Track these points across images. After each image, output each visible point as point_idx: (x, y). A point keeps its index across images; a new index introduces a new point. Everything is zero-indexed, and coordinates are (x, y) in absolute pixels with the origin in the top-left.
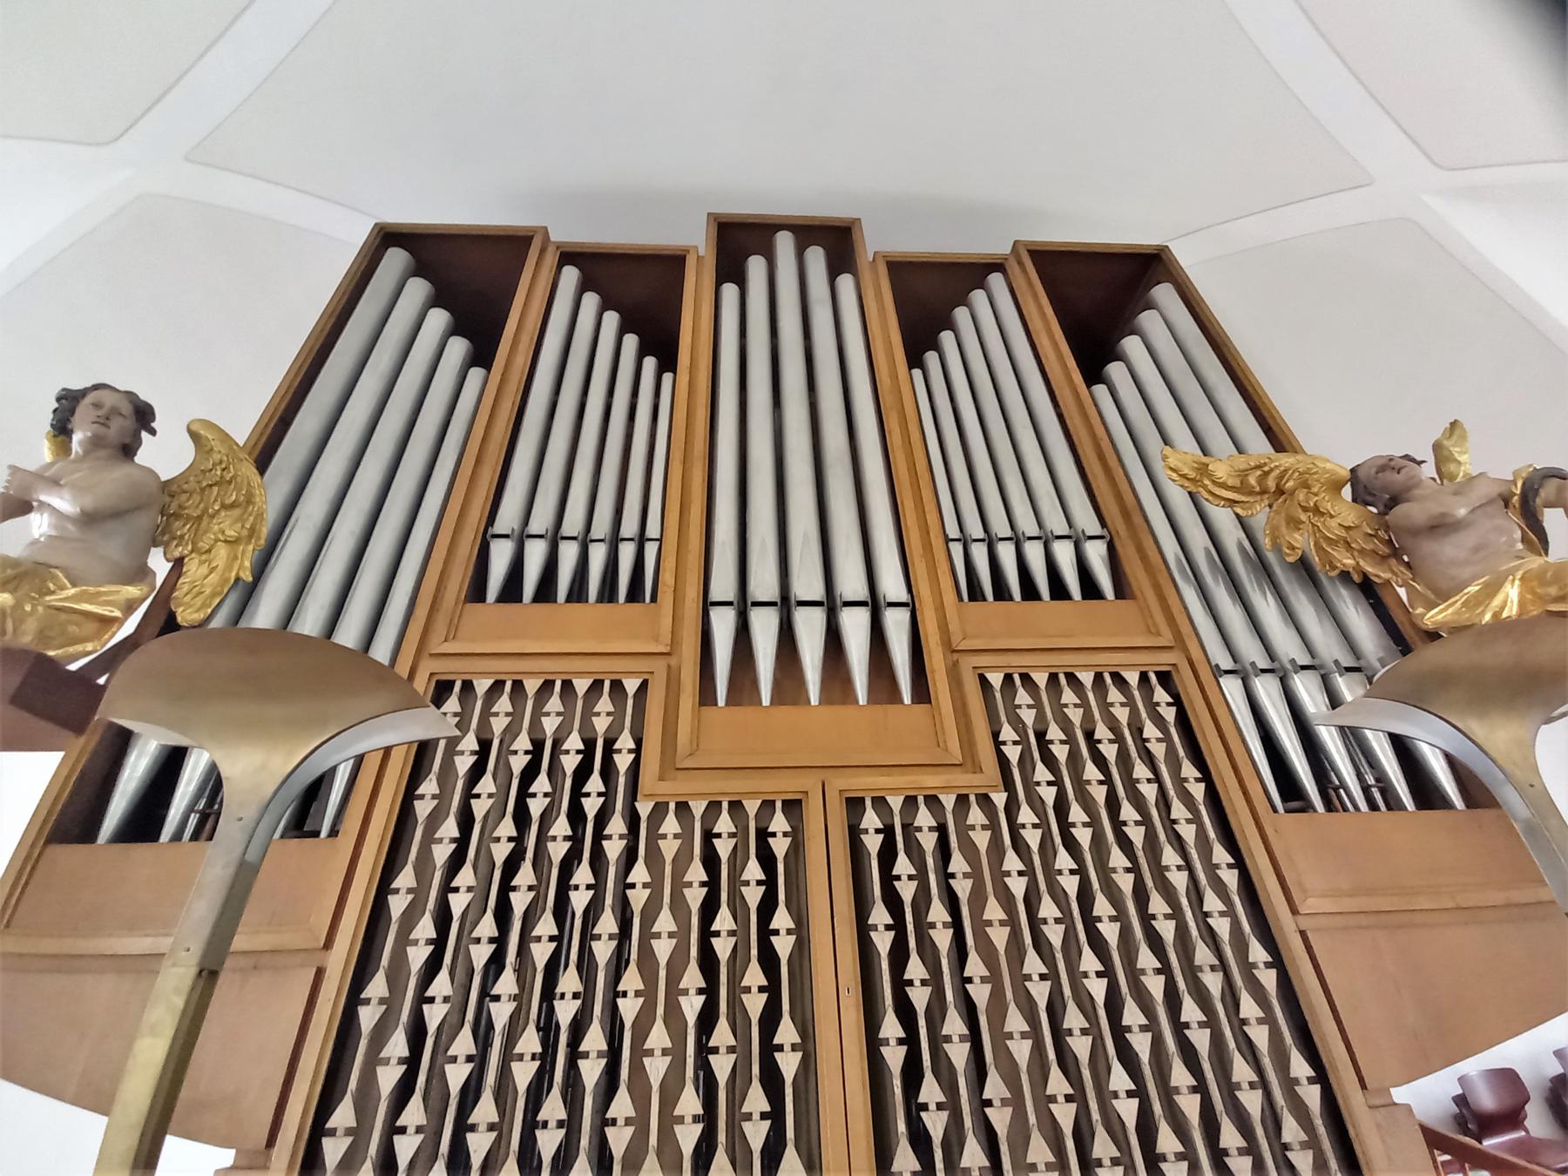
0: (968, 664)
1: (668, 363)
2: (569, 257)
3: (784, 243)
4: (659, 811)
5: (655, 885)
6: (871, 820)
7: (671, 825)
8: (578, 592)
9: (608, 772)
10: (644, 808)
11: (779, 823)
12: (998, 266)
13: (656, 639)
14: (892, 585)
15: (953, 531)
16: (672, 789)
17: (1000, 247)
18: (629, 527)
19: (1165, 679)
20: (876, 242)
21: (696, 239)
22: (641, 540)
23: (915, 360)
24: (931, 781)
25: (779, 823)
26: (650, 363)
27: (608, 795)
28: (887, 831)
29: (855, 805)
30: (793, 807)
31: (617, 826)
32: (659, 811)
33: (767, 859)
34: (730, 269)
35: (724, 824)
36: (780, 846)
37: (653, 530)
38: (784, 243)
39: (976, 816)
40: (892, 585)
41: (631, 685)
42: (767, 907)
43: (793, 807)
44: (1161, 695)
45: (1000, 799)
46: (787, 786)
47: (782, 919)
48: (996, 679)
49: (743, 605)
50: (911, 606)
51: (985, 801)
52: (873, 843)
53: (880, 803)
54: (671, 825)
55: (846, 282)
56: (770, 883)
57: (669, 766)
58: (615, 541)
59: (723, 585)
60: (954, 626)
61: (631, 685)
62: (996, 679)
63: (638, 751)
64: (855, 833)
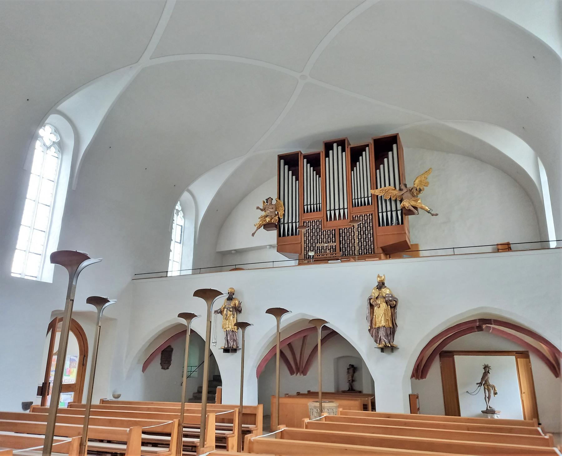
0: (351, 215)
4: (323, 231)
6: (341, 230)
8: (314, 211)
9: (319, 228)
10: (322, 231)
11: (333, 231)
13: (322, 215)
16: (324, 229)
18: (318, 203)
19: (372, 214)
23: (352, 170)
27: (319, 230)
29: (340, 229)
30: (335, 230)
31: (320, 233)
32: (323, 231)
34: (327, 155)
39: (350, 229)
40: (346, 207)
41: (320, 220)
42: (332, 238)
43: (335, 230)
44: (371, 216)
46: (334, 228)
48: (354, 216)
49: (330, 210)
51: (351, 228)
53: (342, 229)
56: (333, 236)
57: (324, 228)
59: (328, 209)
60: (351, 210)
61: (320, 220)
62: (354, 216)
63: (321, 226)
64: (340, 232)
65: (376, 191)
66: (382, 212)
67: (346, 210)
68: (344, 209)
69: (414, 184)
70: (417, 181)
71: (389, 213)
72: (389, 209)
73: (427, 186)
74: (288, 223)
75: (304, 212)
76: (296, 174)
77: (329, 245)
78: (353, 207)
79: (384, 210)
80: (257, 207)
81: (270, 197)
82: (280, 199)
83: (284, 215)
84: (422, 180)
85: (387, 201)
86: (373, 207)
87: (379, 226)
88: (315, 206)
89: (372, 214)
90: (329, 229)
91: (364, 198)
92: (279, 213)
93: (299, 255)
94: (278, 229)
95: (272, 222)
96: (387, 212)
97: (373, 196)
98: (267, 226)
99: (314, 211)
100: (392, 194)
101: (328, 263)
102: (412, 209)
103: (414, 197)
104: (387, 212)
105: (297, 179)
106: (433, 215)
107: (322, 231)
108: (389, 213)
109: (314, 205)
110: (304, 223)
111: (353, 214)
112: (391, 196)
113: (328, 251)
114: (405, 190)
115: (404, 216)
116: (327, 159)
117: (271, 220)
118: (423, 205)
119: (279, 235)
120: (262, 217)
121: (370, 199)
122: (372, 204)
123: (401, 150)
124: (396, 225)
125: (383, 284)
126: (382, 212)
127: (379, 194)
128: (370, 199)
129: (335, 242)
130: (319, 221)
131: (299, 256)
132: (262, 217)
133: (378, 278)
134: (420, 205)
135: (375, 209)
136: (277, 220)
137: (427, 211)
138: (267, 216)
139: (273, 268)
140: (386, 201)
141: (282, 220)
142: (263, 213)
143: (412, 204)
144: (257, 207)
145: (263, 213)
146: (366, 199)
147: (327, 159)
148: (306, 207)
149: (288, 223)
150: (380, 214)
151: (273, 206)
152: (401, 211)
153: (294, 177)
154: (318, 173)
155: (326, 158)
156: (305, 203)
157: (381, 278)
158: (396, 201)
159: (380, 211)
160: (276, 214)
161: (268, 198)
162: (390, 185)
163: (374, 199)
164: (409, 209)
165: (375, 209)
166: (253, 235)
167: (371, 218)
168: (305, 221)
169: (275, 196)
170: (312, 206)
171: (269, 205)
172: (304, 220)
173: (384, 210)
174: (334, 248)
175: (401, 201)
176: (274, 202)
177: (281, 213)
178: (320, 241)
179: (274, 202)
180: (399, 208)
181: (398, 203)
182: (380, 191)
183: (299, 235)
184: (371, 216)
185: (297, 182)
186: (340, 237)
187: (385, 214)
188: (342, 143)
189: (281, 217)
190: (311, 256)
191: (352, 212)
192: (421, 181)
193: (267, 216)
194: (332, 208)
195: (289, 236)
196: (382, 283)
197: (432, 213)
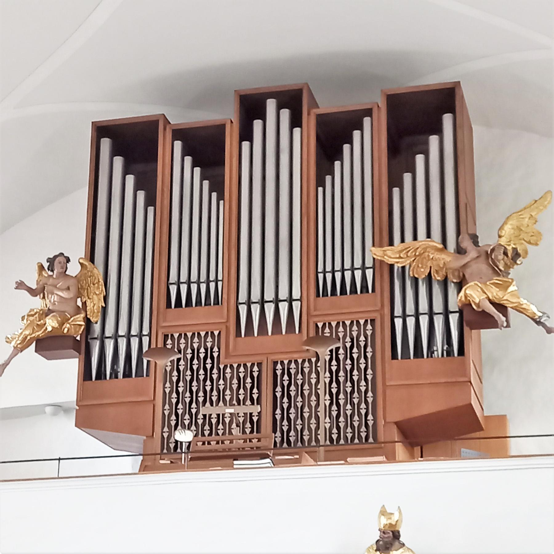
1: (221, 197)
4: (225, 367)
5: (225, 384)
6: (279, 367)
7: (228, 370)
8: (199, 303)
9: (212, 358)
10: (222, 367)
11: (256, 369)
16: (228, 362)
18: (212, 277)
19: (373, 321)
22: (216, 281)
24: (295, 356)
25: (256, 369)
26: (214, 195)
27: (213, 363)
28: (283, 369)
29: (275, 363)
30: (259, 365)
31: (215, 371)
32: (225, 367)
33: (252, 377)
35: (242, 369)
36: (255, 374)
39: (307, 364)
40: (296, 294)
41: (216, 333)
42: (252, 388)
43: (259, 365)
44: (369, 327)
45: (314, 360)
47: (255, 391)
48: (320, 325)
49: (249, 303)
51: (310, 361)
52: (279, 372)
53: (282, 363)
54: (228, 370)
55: (297, 131)
56: (253, 383)
57: (227, 355)
58: (208, 282)
59: (243, 297)
60: (312, 307)
61: (216, 333)
62: (320, 325)
63: (219, 352)
64: (275, 370)
66: (404, 317)
67: (296, 305)
68: (290, 300)
69: (500, 237)
70: (508, 228)
71: (424, 321)
72: (424, 306)
73: (537, 244)
74: (116, 337)
75: (169, 305)
77: (242, 410)
78: (318, 295)
80: (17, 282)
81: (62, 254)
82: (92, 259)
83: (104, 310)
84: (522, 225)
85: (420, 283)
87: (394, 356)
88: (203, 287)
89: (373, 321)
90: (242, 360)
92: (88, 304)
93: (145, 438)
94: (83, 356)
96: (417, 315)
97: (377, 265)
99: (199, 303)
100: (435, 263)
101: (231, 467)
102: (492, 310)
103: (499, 275)
104: (417, 315)
105: (150, 201)
107: (222, 367)
108: (424, 321)
109: (199, 283)
110: (166, 337)
111: (316, 319)
112: (431, 267)
114: (472, 253)
115: (466, 329)
117: (62, 324)
118: (523, 301)
119: (86, 374)
120: (33, 315)
121: (369, 273)
122: (373, 290)
123: (465, 132)
124: (443, 355)
125: (396, 535)
126: (404, 317)
127: (397, 260)
128: (369, 273)
131: (144, 441)
132: (33, 315)
133: (379, 518)
134: (514, 301)
135: (382, 306)
136: (81, 325)
137: (533, 319)
138: (47, 313)
139: (59, 478)
140: (415, 281)
141: (97, 328)
142: (37, 303)
143: (491, 298)
144: (17, 282)
145: (37, 303)
146: (358, 274)
148: (173, 290)
149: (116, 337)
150: (398, 323)
151: (71, 283)
153: (141, 195)
157: (390, 518)
158: (445, 284)
159: (398, 311)
160: (79, 307)
161: (55, 257)
162: (429, 236)
163: (382, 276)
164: (483, 311)
165: (382, 306)
167: (369, 333)
168: (169, 332)
170: (194, 287)
171: (58, 278)
172: (166, 331)
174: (255, 419)
175: (460, 286)
176: (73, 269)
178: (214, 399)
179: (73, 269)
180: (453, 305)
181: (452, 289)
182: (401, 251)
184: (369, 327)
185: (151, 209)
186: (275, 386)
187: (411, 322)
189: (96, 319)
190: (181, 443)
192: (519, 229)
193: (47, 313)
194: (256, 296)
195: (117, 377)
196: (391, 533)
197: (548, 324)
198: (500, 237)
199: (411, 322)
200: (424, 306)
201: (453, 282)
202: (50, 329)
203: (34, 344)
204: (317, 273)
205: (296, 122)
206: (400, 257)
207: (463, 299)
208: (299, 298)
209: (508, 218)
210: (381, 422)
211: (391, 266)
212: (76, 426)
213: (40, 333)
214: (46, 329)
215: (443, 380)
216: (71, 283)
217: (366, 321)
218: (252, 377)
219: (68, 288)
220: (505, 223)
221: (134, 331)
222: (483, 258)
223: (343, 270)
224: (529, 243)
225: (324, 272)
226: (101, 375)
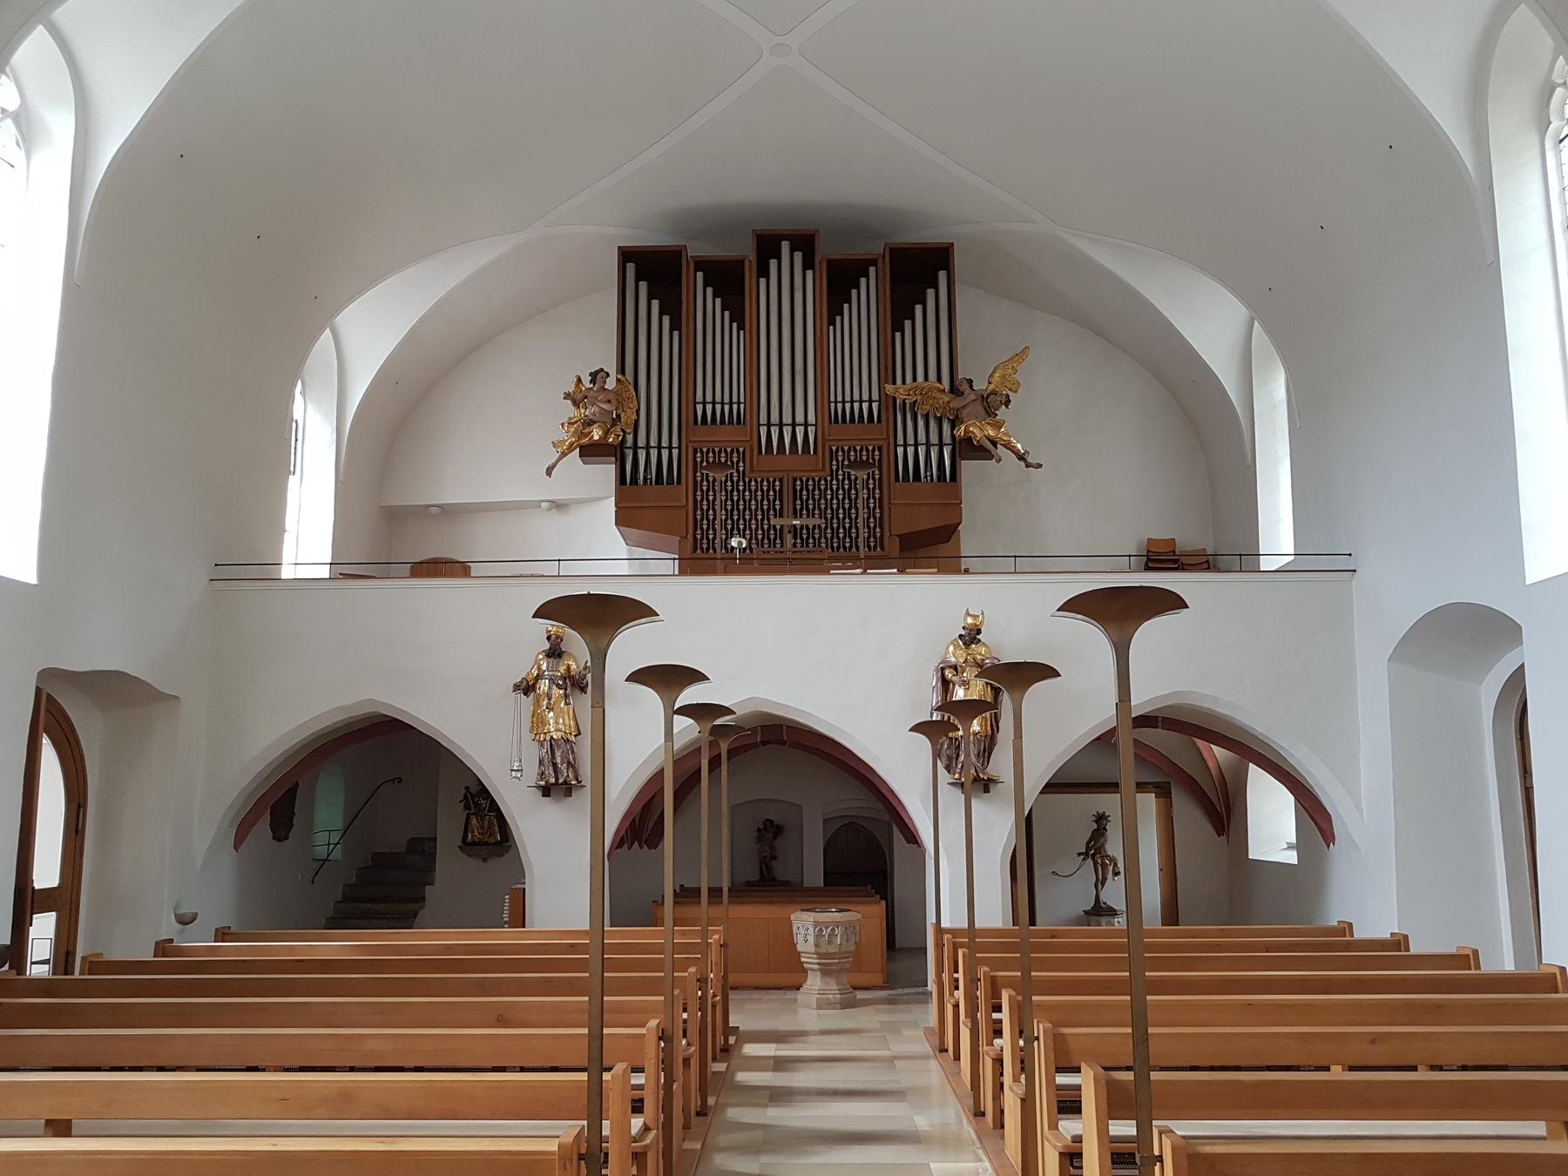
0: (827, 444)
2: (701, 264)
3: (785, 246)
4: (750, 481)
6: (798, 483)
8: (723, 422)
10: (747, 480)
11: (777, 483)
12: (874, 262)
14: (811, 418)
15: (832, 399)
17: (876, 248)
19: (880, 449)
20: (824, 251)
21: (746, 250)
22: (739, 403)
34: (763, 272)
37: (742, 400)
38: (785, 246)
40: (811, 418)
41: (741, 450)
42: (774, 500)
43: (781, 480)
44: (877, 453)
45: (829, 479)
48: (834, 448)
50: (816, 425)
51: (826, 480)
55: (809, 273)
57: (752, 470)
58: (731, 403)
59: (763, 420)
61: (741, 450)
62: (834, 448)
65: (901, 391)
66: (905, 445)
67: (811, 430)
69: (990, 383)
72: (922, 437)
73: (1016, 392)
74: (648, 447)
76: (673, 308)
78: (830, 422)
79: (911, 440)
80: (565, 393)
82: (623, 372)
83: (637, 422)
85: (919, 417)
86: (885, 429)
88: (727, 408)
89: (880, 449)
90: (765, 475)
91: (861, 401)
92: (622, 416)
93: (678, 538)
95: (611, 440)
97: (883, 398)
98: (590, 452)
99: (723, 422)
103: (990, 416)
104: (916, 445)
106: (1028, 465)
107: (747, 480)
109: (723, 404)
110: (695, 451)
111: (831, 443)
113: (789, 539)
116: (763, 281)
117: (606, 433)
120: (573, 423)
121: (875, 406)
122: (879, 421)
126: (905, 445)
128: (875, 406)
129: (781, 516)
130: (738, 451)
131: (680, 541)
132: (573, 423)
136: (619, 436)
138: (589, 423)
141: (630, 438)
146: (865, 406)
147: (763, 281)
148: (699, 408)
149: (648, 447)
152: (951, 447)
154: (738, 317)
155: (759, 277)
156: (699, 397)
158: (939, 421)
159: (900, 441)
166: (549, 471)
169: (611, 368)
170: (718, 407)
171: (598, 391)
173: (911, 440)
176: (611, 384)
177: (628, 417)
179: (611, 384)
180: (947, 438)
183: (679, 482)
184: (877, 453)
185: (676, 333)
186: (795, 500)
188: (805, 243)
191: (829, 435)
192: (1003, 377)
193: (589, 423)
195: (636, 484)
198: (990, 383)
199: (910, 450)
200: (922, 437)
201: (948, 418)
202: (596, 438)
203: (578, 449)
204: (830, 402)
205: (808, 264)
206: (909, 395)
207: (962, 434)
208: (814, 423)
209: (996, 368)
210: (887, 534)
211: (895, 399)
212: (616, 524)
213: (585, 441)
214: (592, 437)
215: (940, 502)
216: (611, 397)
217: (874, 447)
218: (774, 491)
219: (609, 401)
220: (994, 371)
221: (665, 443)
222: (980, 400)
223: (852, 401)
224: (1010, 390)
225: (836, 402)
226: (634, 480)
